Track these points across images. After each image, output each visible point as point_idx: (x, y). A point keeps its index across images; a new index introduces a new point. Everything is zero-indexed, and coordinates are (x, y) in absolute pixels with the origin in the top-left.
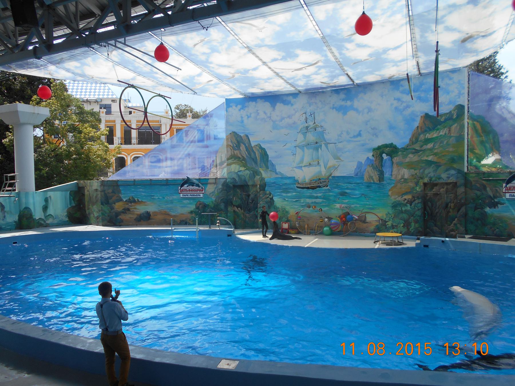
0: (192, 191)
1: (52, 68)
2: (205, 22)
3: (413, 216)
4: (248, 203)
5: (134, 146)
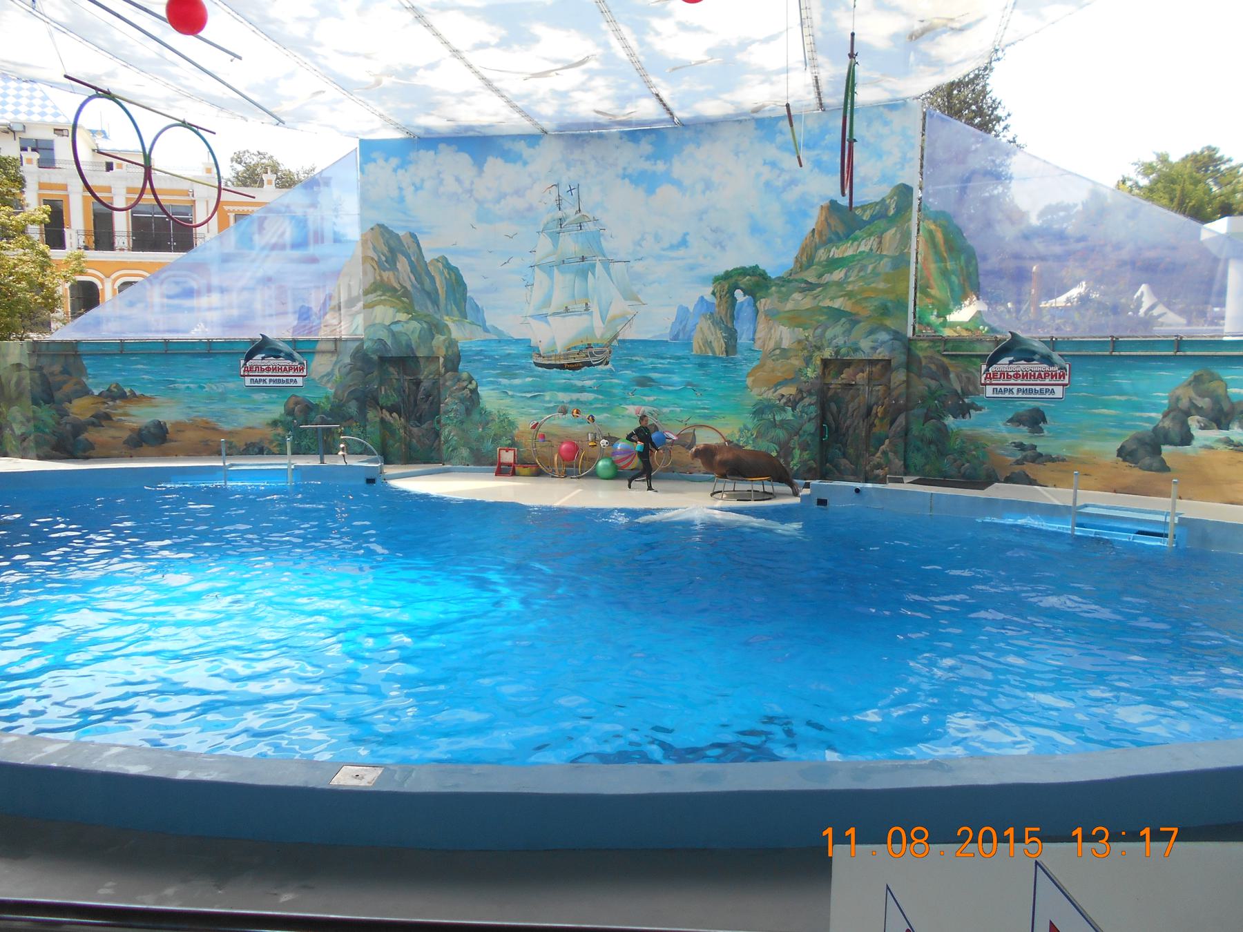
0: (274, 369)
3: (797, 433)
4: (415, 401)
5: (124, 253)
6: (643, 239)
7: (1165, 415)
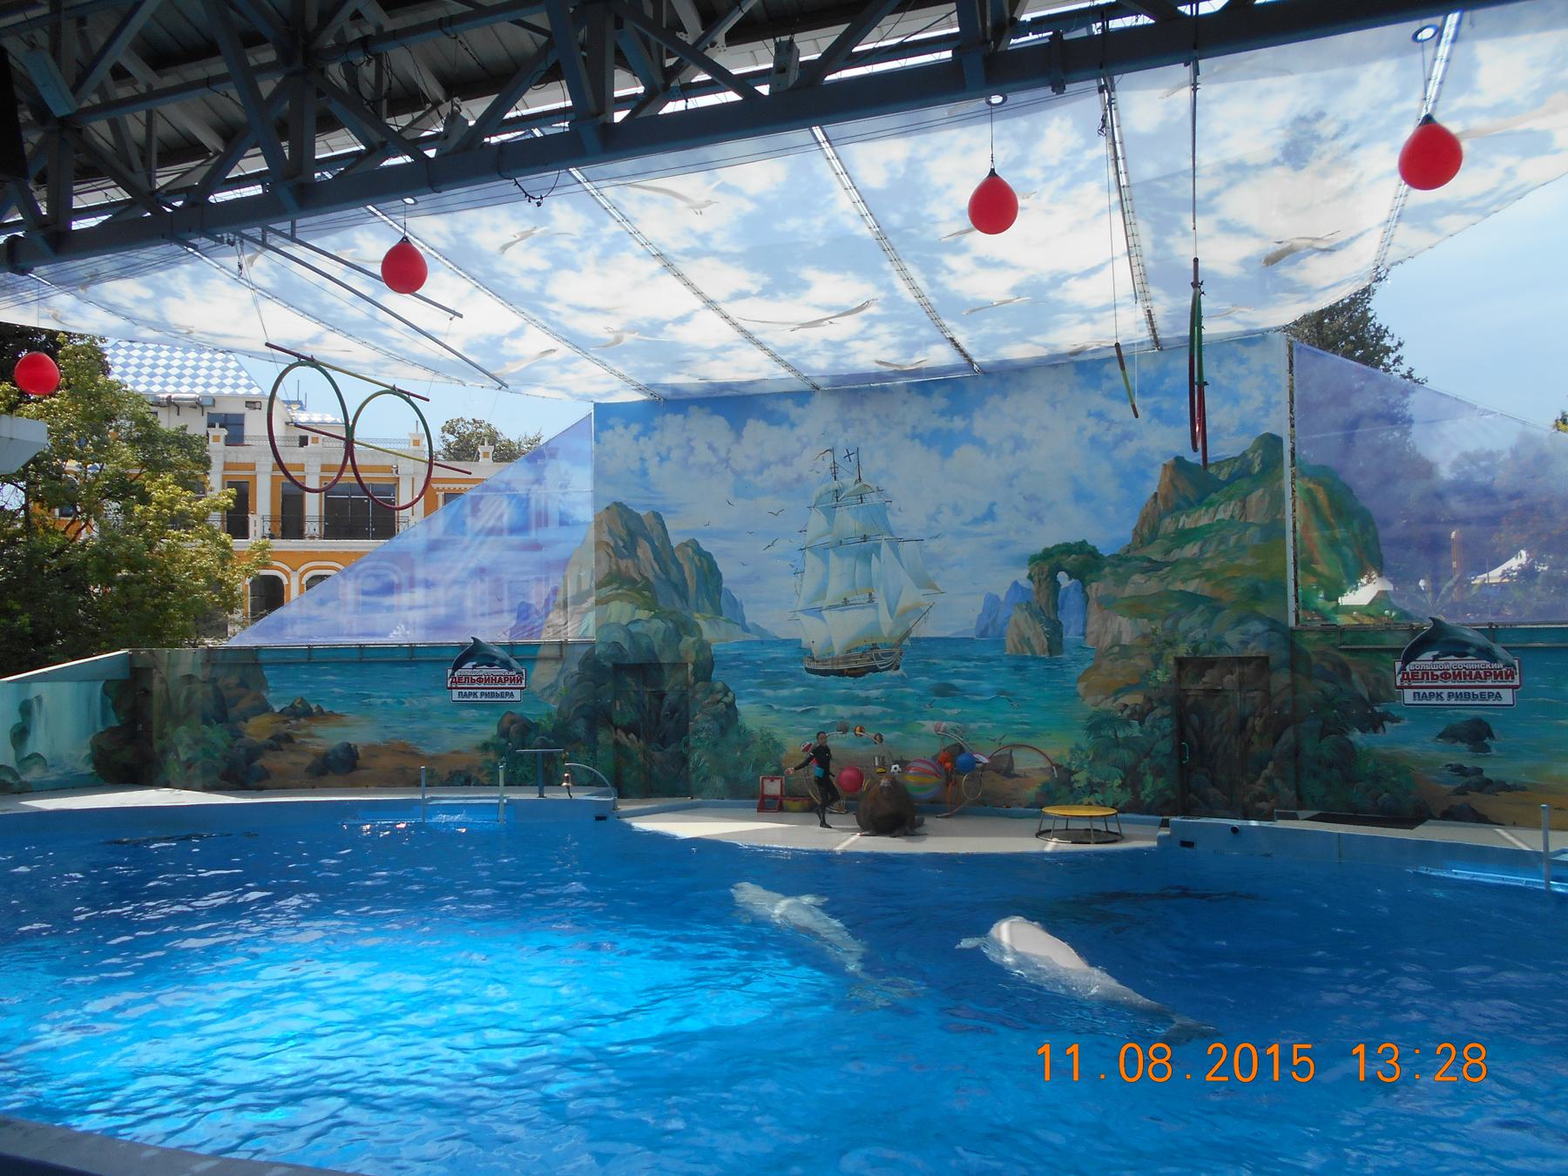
0: (487, 680)
1: (63, 300)
2: (532, 181)
3: (1147, 755)
4: (658, 715)
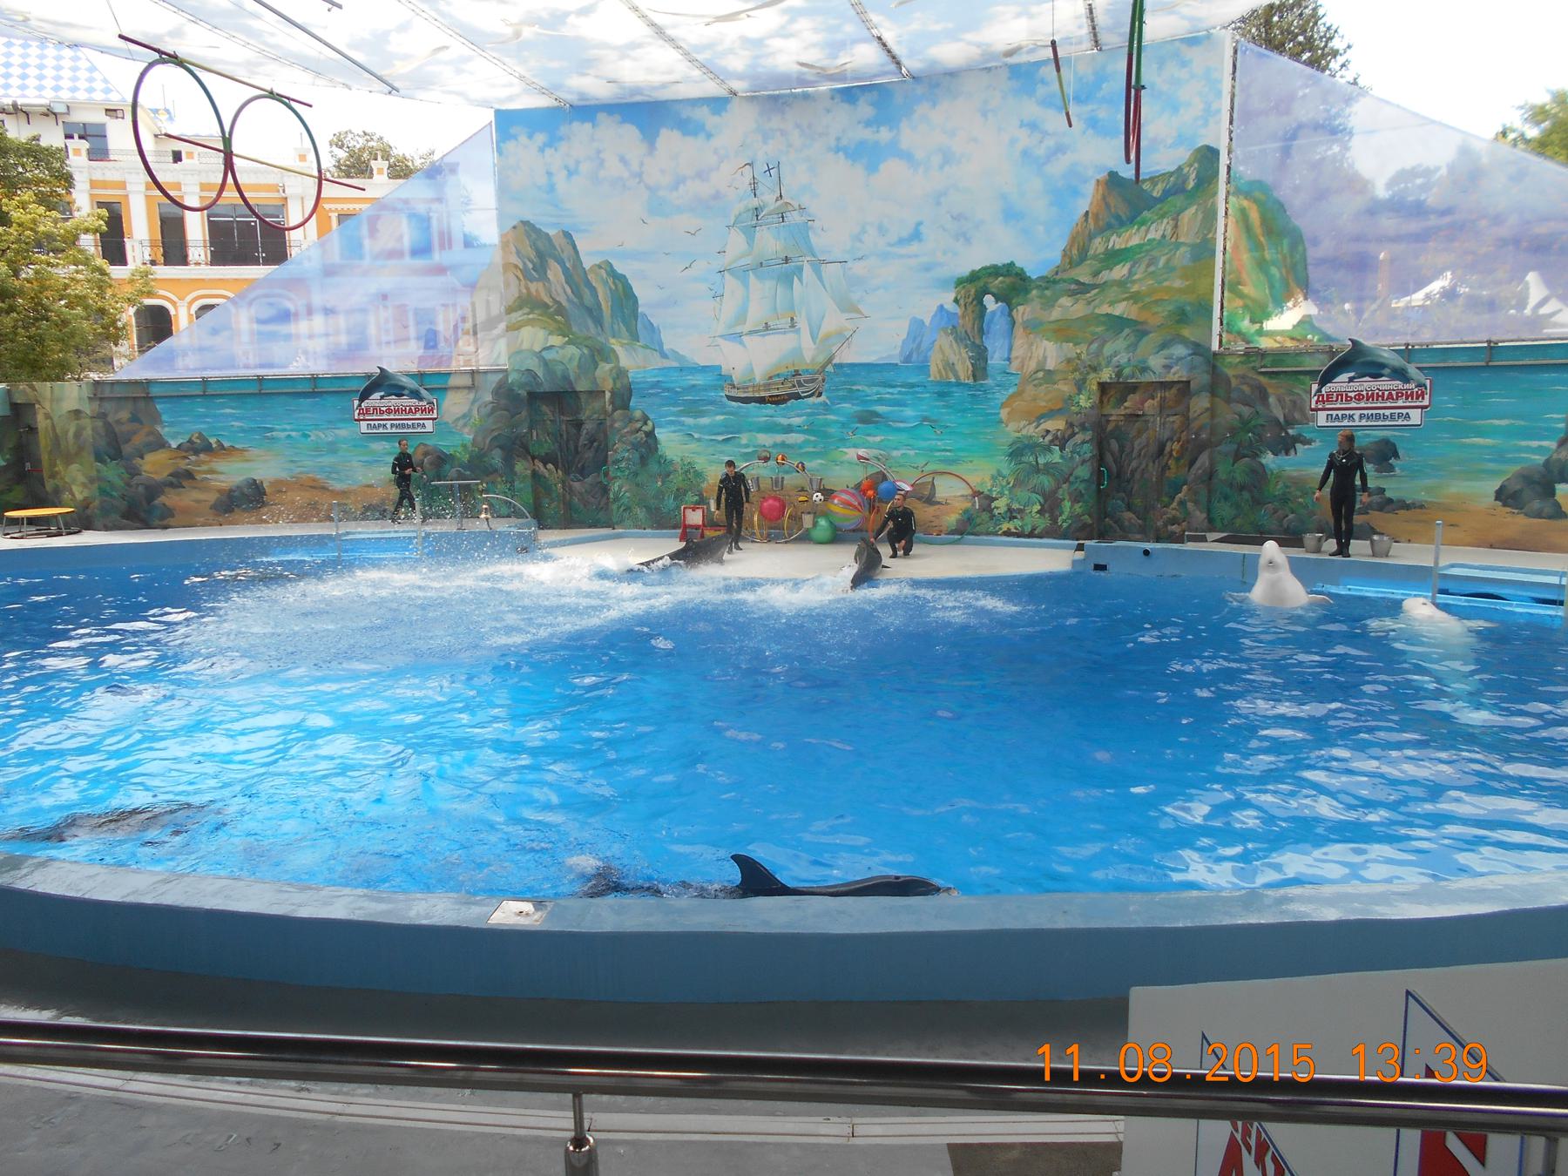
3: (1066, 480)
6: (864, 231)
7: (1562, 443)
